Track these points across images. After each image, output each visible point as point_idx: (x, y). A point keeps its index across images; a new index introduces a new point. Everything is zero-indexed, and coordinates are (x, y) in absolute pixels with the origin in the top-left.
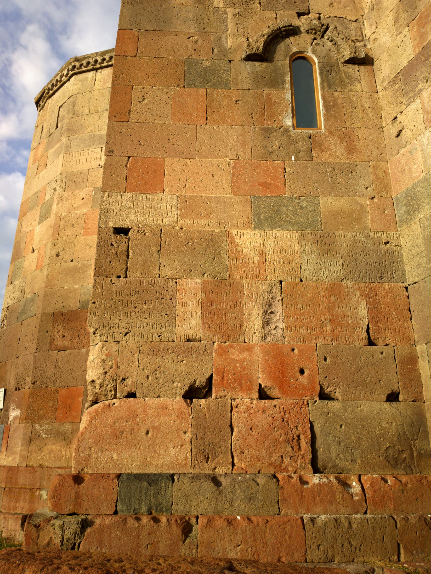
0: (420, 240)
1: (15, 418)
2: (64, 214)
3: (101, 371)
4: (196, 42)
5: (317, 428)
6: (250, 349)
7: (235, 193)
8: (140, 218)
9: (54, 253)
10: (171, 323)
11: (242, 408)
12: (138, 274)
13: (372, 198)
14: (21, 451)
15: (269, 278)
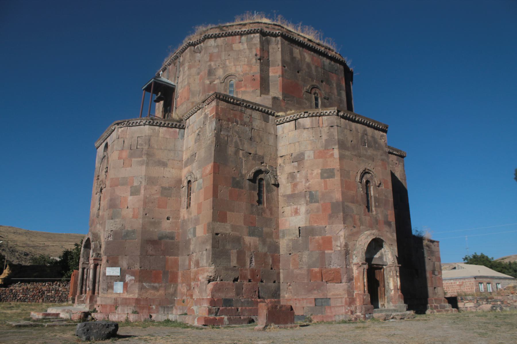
0: (285, 244)
1: (131, 280)
2: (148, 196)
3: (214, 274)
4: (235, 170)
5: (260, 288)
6: (247, 270)
7: (244, 225)
8: (221, 231)
9: (145, 214)
10: (230, 262)
11: (245, 284)
12: (222, 248)
13: (275, 229)
14: (138, 292)
15: (251, 251)
